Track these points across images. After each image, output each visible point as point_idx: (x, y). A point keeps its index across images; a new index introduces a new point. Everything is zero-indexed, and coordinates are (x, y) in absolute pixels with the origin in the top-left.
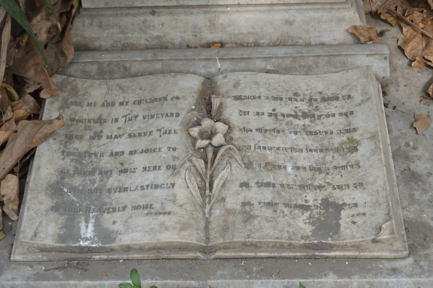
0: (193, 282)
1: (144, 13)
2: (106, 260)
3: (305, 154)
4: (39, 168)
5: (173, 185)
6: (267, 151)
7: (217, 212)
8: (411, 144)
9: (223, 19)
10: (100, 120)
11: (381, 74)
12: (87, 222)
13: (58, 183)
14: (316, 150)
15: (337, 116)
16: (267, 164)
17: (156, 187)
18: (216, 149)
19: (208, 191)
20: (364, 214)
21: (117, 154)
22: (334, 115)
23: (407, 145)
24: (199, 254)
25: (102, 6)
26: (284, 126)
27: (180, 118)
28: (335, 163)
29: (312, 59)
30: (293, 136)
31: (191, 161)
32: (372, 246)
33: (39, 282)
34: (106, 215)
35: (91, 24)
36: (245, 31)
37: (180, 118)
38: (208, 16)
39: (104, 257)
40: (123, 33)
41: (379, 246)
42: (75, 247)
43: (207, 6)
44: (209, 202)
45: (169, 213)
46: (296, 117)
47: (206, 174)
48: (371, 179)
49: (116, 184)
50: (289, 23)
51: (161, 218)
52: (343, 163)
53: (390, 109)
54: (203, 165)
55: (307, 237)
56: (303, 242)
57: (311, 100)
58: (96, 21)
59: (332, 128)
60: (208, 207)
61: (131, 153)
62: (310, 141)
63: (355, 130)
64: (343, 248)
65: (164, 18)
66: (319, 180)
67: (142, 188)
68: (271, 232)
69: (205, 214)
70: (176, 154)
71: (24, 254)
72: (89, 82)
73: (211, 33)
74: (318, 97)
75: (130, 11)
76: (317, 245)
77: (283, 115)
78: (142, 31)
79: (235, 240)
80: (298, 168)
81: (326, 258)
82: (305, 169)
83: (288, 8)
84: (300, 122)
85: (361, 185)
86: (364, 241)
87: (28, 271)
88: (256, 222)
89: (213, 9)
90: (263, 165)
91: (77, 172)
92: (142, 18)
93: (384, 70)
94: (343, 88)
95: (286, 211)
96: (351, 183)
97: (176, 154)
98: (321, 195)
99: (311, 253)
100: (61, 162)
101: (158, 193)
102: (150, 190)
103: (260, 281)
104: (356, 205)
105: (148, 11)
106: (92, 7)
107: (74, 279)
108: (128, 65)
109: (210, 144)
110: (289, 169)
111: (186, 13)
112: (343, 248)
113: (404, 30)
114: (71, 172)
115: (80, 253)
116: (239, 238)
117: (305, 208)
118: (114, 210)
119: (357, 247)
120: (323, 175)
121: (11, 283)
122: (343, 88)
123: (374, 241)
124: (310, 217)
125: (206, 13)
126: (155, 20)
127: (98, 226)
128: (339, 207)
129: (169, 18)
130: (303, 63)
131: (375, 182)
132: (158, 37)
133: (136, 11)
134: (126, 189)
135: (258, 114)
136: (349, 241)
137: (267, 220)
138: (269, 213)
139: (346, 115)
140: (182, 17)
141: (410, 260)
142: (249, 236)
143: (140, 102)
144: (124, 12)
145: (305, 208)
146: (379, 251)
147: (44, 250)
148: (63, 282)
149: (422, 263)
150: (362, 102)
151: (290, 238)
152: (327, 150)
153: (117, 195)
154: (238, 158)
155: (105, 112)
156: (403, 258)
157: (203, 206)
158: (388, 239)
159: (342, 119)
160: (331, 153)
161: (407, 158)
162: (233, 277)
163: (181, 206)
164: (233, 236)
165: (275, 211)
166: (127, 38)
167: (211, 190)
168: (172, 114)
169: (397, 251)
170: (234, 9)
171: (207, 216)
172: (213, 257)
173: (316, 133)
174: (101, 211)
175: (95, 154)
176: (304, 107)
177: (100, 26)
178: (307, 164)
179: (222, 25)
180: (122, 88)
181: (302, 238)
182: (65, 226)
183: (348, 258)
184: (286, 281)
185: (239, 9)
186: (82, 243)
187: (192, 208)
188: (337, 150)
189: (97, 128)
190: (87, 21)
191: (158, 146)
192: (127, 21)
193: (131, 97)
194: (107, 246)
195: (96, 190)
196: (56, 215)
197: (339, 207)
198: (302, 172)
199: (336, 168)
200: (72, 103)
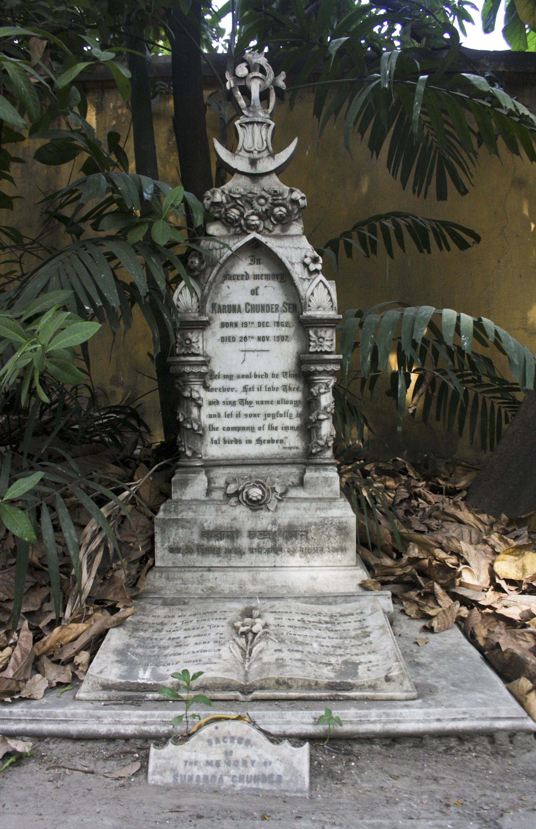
0: (232, 713)
1: (203, 571)
2: (157, 700)
3: (327, 639)
4: (109, 640)
5: (219, 650)
6: (297, 636)
7: (255, 666)
8: (415, 650)
9: (263, 575)
10: (162, 624)
11: (387, 609)
12: (145, 670)
13: (123, 649)
14: (337, 638)
15: (353, 622)
16: (296, 642)
17: (205, 651)
18: (255, 634)
19: (247, 656)
20: (378, 665)
21: (174, 639)
22: (350, 622)
23: (412, 651)
24: (238, 694)
25: (170, 565)
26: (310, 626)
27: (227, 621)
28: (353, 644)
29: (331, 598)
30: (318, 631)
31: (234, 640)
32: (385, 685)
33: (98, 711)
34: (161, 667)
35: (161, 577)
36: (279, 585)
37: (227, 621)
38: (251, 573)
39: (157, 695)
40: (184, 583)
41: (392, 685)
42: (134, 683)
43: (250, 567)
44: (249, 661)
45: (215, 663)
46: (320, 623)
47: (247, 648)
48: (382, 647)
49: (171, 652)
50: (314, 579)
51: (208, 666)
52: (360, 643)
53: (397, 636)
54: (244, 642)
55: (331, 678)
56: (327, 680)
57: (331, 616)
58: (164, 575)
59: (349, 628)
60: (247, 665)
61: (185, 637)
62: (332, 634)
63: (367, 627)
64: (361, 687)
65: (217, 574)
66: (339, 651)
67: (194, 652)
68: (301, 673)
69: (244, 668)
70: (222, 636)
71: (88, 692)
72: (155, 606)
73: (253, 585)
74: (338, 615)
75: (192, 569)
76: (339, 684)
77: (310, 622)
78: (199, 583)
79: (270, 676)
80: (322, 646)
81: (348, 699)
82: (328, 647)
83: (312, 568)
84: (324, 626)
85: (374, 652)
86: (377, 679)
87: (89, 705)
88: (288, 668)
89: (255, 569)
90: (293, 642)
91: (139, 646)
92: (200, 574)
93: (389, 606)
94: (357, 609)
95: (313, 664)
96: (366, 652)
97: (222, 636)
98: (341, 660)
99: (334, 693)
100: (128, 640)
101: (206, 654)
102: (199, 653)
103: (291, 712)
104: (371, 662)
105: (205, 569)
106: (163, 565)
107: (129, 710)
108: (186, 601)
109: (251, 631)
110: (315, 645)
111: (234, 571)
112: (361, 687)
113: (404, 603)
114: (136, 646)
115: (137, 691)
116: (274, 674)
117: (329, 664)
118: (169, 664)
119: (373, 687)
120: (343, 650)
121: (72, 711)
122: (357, 609)
123: (388, 679)
124: (333, 669)
125: (250, 571)
126: (211, 575)
127: (153, 672)
128: (356, 665)
129: (221, 573)
130: (325, 601)
131: (385, 648)
132: (211, 588)
133: (196, 569)
134: (180, 654)
135: (289, 619)
136: (366, 680)
137: (297, 667)
138: (299, 664)
139: (360, 621)
140: (231, 573)
141: (420, 701)
142: (281, 674)
143: (195, 615)
144: (186, 569)
145: (329, 664)
146: (392, 691)
147: (106, 687)
148: (119, 712)
149: (429, 702)
150: (372, 613)
151: (316, 677)
152: (345, 638)
153: (172, 657)
154: (273, 637)
155: (166, 620)
156: (414, 699)
157: (243, 664)
158: (398, 676)
159: (358, 623)
160: (349, 640)
161: (412, 656)
162: (267, 710)
163: (225, 660)
164: (268, 674)
165: (304, 664)
166: (187, 588)
167: (250, 655)
168: (220, 619)
169: (407, 691)
170: (271, 569)
171: (246, 669)
172: (250, 697)
173: (336, 631)
174: (158, 665)
175: (156, 639)
176: (327, 619)
177: (168, 579)
178: (329, 644)
179: (262, 579)
180: (181, 610)
181: (326, 678)
182: (127, 671)
183: (367, 699)
184: (314, 712)
185: (276, 569)
186: (140, 681)
187: (234, 663)
188: (354, 638)
189: (160, 627)
190: (158, 575)
191: (208, 633)
192: (188, 575)
193: (188, 613)
194: (160, 682)
195: (155, 656)
196: (119, 665)
197: (356, 665)
198: (325, 648)
199: (353, 646)
200: (140, 614)
